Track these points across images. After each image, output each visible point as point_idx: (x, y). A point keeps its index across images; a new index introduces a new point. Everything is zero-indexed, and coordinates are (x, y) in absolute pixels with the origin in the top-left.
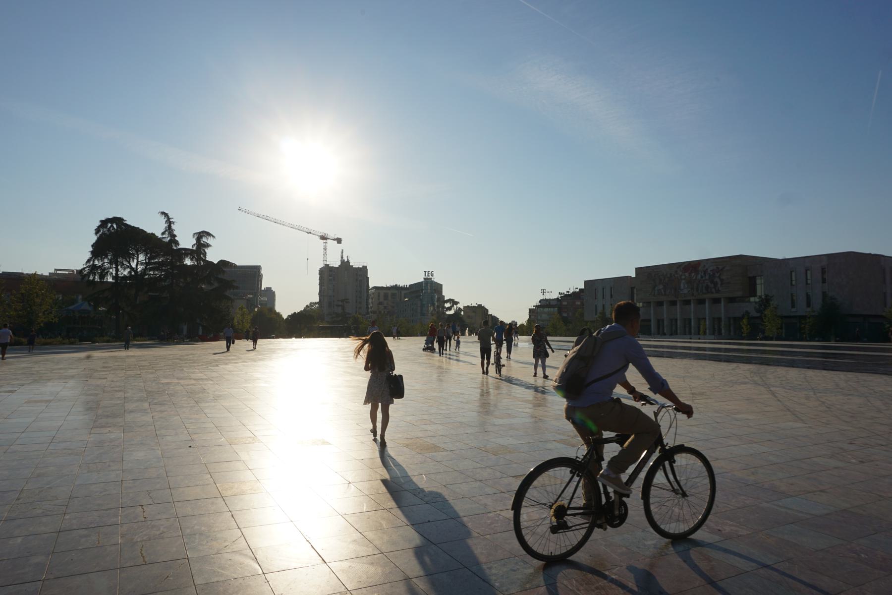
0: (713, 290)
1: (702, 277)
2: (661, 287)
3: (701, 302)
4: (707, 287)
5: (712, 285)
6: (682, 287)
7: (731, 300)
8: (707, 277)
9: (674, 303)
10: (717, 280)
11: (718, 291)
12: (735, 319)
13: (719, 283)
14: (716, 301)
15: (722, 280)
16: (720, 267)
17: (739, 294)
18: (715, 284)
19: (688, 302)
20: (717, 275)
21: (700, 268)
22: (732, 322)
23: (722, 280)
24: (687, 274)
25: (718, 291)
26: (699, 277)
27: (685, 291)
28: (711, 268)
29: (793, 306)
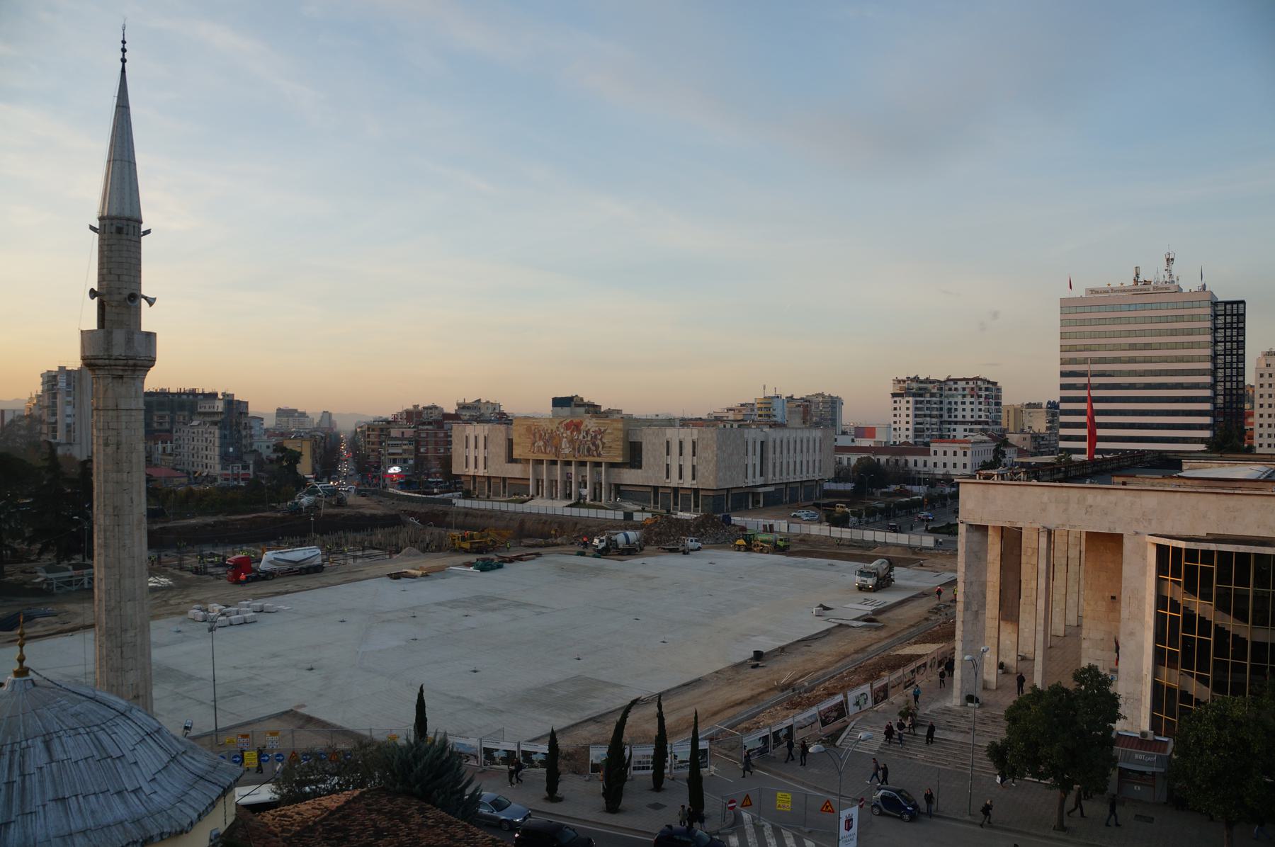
2: (541, 443)
3: (583, 464)
4: (589, 450)
7: (612, 465)
9: (554, 463)
10: (598, 442)
11: (599, 455)
14: (598, 464)
17: (620, 460)
18: (597, 447)
19: (568, 463)
25: (599, 455)
27: (567, 451)
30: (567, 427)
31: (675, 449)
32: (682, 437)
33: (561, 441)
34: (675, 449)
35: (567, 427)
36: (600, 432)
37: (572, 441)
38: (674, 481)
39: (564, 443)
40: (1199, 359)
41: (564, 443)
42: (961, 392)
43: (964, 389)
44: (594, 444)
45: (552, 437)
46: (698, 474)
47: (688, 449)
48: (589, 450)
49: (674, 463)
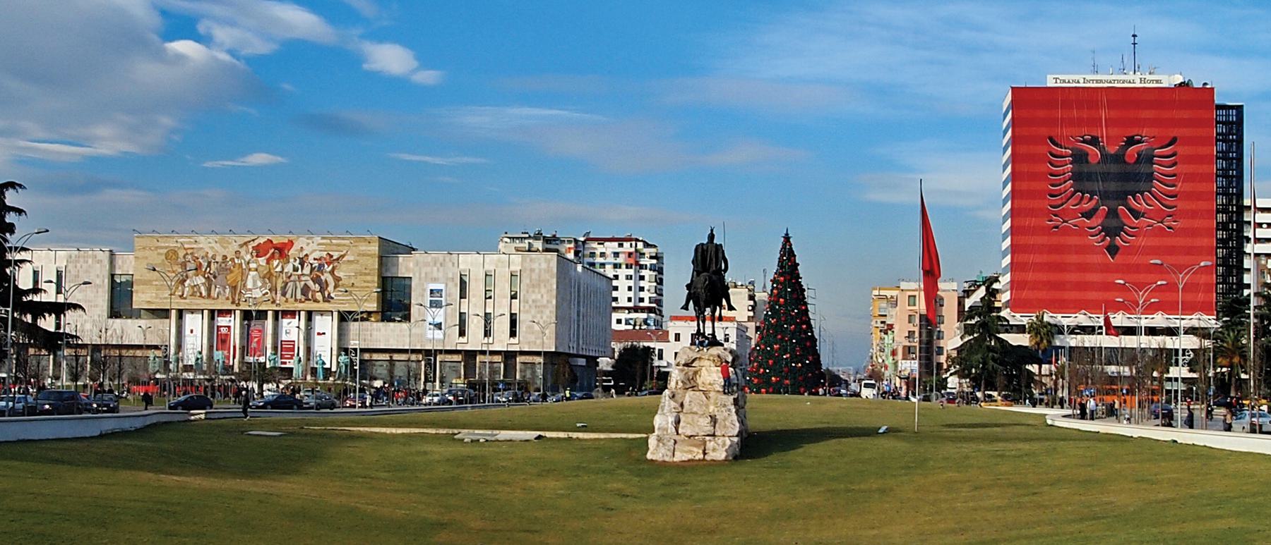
0: (319, 296)
1: (296, 269)
2: (200, 280)
4: (305, 290)
5: (317, 287)
6: (250, 285)
8: (307, 270)
10: (326, 277)
11: (328, 299)
15: (337, 279)
18: (323, 286)
23: (337, 279)
24: (262, 261)
25: (328, 299)
26: (289, 268)
27: (257, 294)
28: (317, 255)
29: (462, 333)
30: (259, 251)
32: (489, 267)
35: (259, 251)
36: (331, 260)
37: (268, 276)
38: (474, 340)
40: (1205, 178)
42: (611, 259)
43: (616, 255)
44: (317, 280)
46: (521, 328)
48: (305, 290)
49: (474, 306)
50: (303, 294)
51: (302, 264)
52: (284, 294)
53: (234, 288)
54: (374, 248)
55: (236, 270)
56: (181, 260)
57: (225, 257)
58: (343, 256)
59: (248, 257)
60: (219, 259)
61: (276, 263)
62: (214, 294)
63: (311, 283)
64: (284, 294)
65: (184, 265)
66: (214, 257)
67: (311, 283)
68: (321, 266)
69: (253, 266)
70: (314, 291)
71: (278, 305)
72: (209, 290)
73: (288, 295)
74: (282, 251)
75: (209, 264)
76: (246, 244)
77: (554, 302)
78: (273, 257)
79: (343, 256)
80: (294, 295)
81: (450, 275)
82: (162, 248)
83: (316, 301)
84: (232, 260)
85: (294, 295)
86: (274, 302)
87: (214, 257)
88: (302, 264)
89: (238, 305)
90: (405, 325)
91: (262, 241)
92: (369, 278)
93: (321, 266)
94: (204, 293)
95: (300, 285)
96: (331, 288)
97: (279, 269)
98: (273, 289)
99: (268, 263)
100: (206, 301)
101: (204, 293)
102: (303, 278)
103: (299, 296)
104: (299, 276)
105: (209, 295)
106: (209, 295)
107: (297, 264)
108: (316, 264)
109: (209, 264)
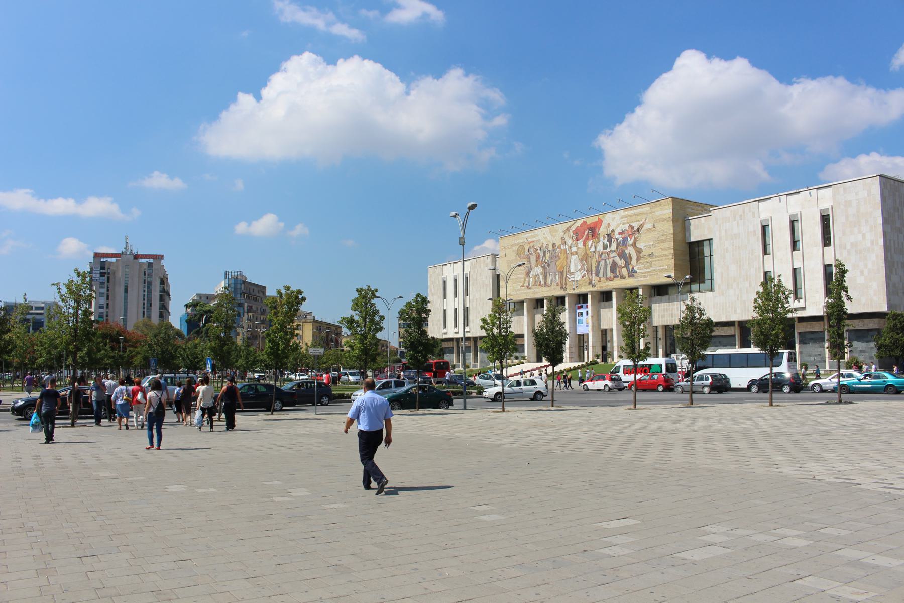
0: (625, 272)
1: (605, 247)
2: (539, 270)
4: (614, 266)
5: (621, 263)
6: (572, 270)
8: (614, 246)
10: (630, 250)
11: (632, 274)
12: (666, 327)
13: (634, 257)
16: (636, 225)
18: (628, 260)
20: (630, 241)
21: (601, 230)
22: (661, 333)
23: (639, 251)
25: (632, 274)
26: (600, 247)
27: (578, 276)
31: (780, 237)
33: (568, 260)
34: (780, 237)
37: (585, 258)
39: (575, 264)
41: (575, 264)
44: (622, 255)
45: (555, 257)
47: (811, 232)
48: (614, 266)
50: (613, 271)
51: (610, 241)
52: (597, 274)
53: (562, 273)
54: (667, 211)
55: (562, 256)
56: (527, 253)
57: (554, 245)
58: (642, 226)
59: (569, 242)
60: (551, 248)
61: (590, 243)
62: (549, 282)
63: (617, 259)
64: (597, 274)
65: (529, 258)
66: (547, 247)
67: (617, 259)
68: (625, 239)
69: (574, 249)
70: (621, 267)
71: (594, 286)
72: (545, 278)
73: (601, 275)
74: (593, 230)
75: (544, 255)
76: (568, 229)
77: (881, 241)
78: (587, 238)
79: (642, 226)
80: (605, 273)
81: (751, 229)
82: (515, 245)
83: (623, 277)
84: (559, 247)
85: (605, 273)
86: (590, 283)
87: (547, 247)
88: (610, 241)
89: (565, 289)
90: (710, 294)
91: (579, 223)
92: (666, 245)
93: (625, 239)
94: (542, 282)
95: (609, 262)
96: (634, 262)
97: (592, 249)
98: (589, 271)
99: (584, 244)
100: (545, 289)
101: (542, 282)
102: (612, 255)
103: (609, 274)
104: (608, 254)
105: (545, 283)
106: (545, 283)
107: (606, 241)
108: (620, 238)
109: (544, 255)
